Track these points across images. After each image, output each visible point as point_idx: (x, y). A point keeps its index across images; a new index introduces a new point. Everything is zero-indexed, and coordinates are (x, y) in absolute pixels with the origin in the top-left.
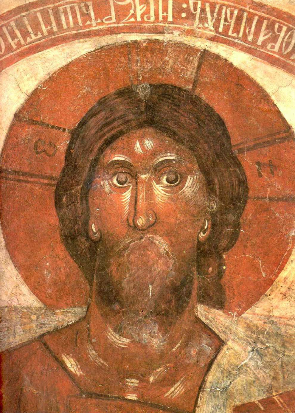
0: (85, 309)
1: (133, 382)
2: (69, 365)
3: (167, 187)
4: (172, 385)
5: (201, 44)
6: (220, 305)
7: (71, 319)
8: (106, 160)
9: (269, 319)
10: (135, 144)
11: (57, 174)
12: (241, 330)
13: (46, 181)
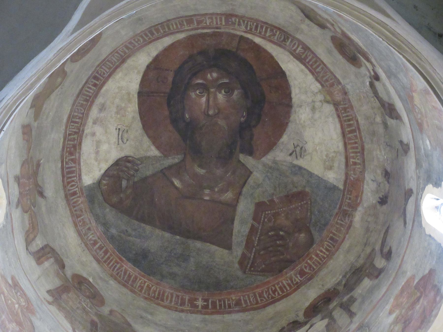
0: (183, 156)
1: (207, 191)
2: (176, 183)
3: (224, 95)
4: (226, 193)
5: (238, 33)
6: (250, 152)
7: (176, 161)
8: (193, 82)
9: (275, 162)
10: (208, 75)
11: (168, 91)
12: (260, 167)
13: (162, 95)
